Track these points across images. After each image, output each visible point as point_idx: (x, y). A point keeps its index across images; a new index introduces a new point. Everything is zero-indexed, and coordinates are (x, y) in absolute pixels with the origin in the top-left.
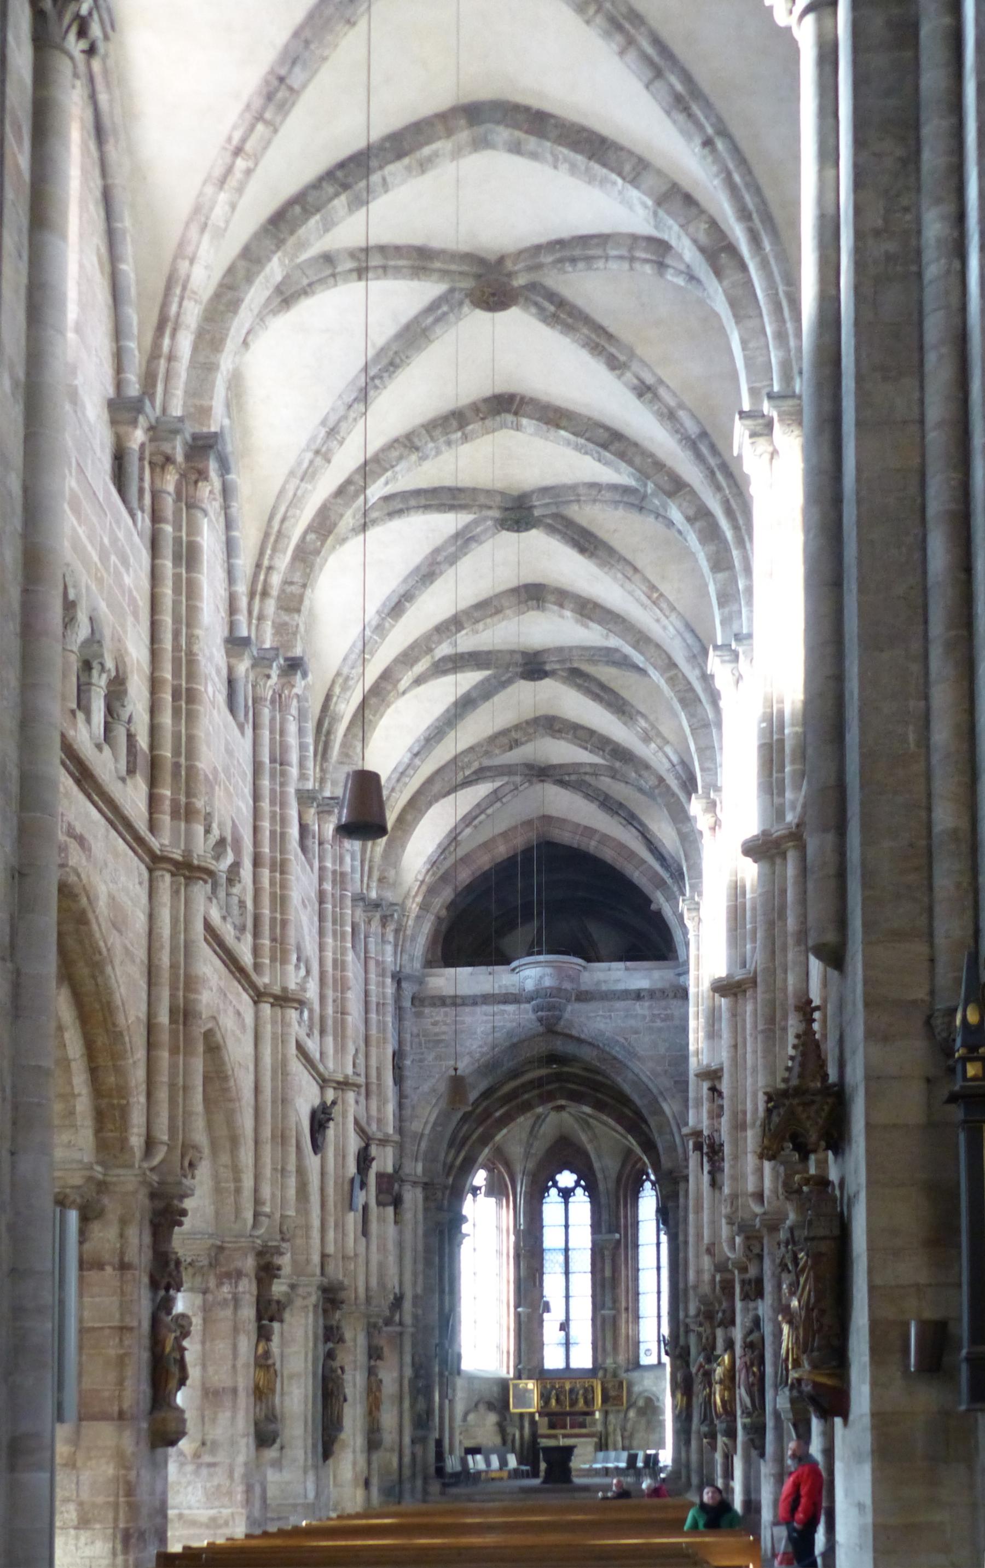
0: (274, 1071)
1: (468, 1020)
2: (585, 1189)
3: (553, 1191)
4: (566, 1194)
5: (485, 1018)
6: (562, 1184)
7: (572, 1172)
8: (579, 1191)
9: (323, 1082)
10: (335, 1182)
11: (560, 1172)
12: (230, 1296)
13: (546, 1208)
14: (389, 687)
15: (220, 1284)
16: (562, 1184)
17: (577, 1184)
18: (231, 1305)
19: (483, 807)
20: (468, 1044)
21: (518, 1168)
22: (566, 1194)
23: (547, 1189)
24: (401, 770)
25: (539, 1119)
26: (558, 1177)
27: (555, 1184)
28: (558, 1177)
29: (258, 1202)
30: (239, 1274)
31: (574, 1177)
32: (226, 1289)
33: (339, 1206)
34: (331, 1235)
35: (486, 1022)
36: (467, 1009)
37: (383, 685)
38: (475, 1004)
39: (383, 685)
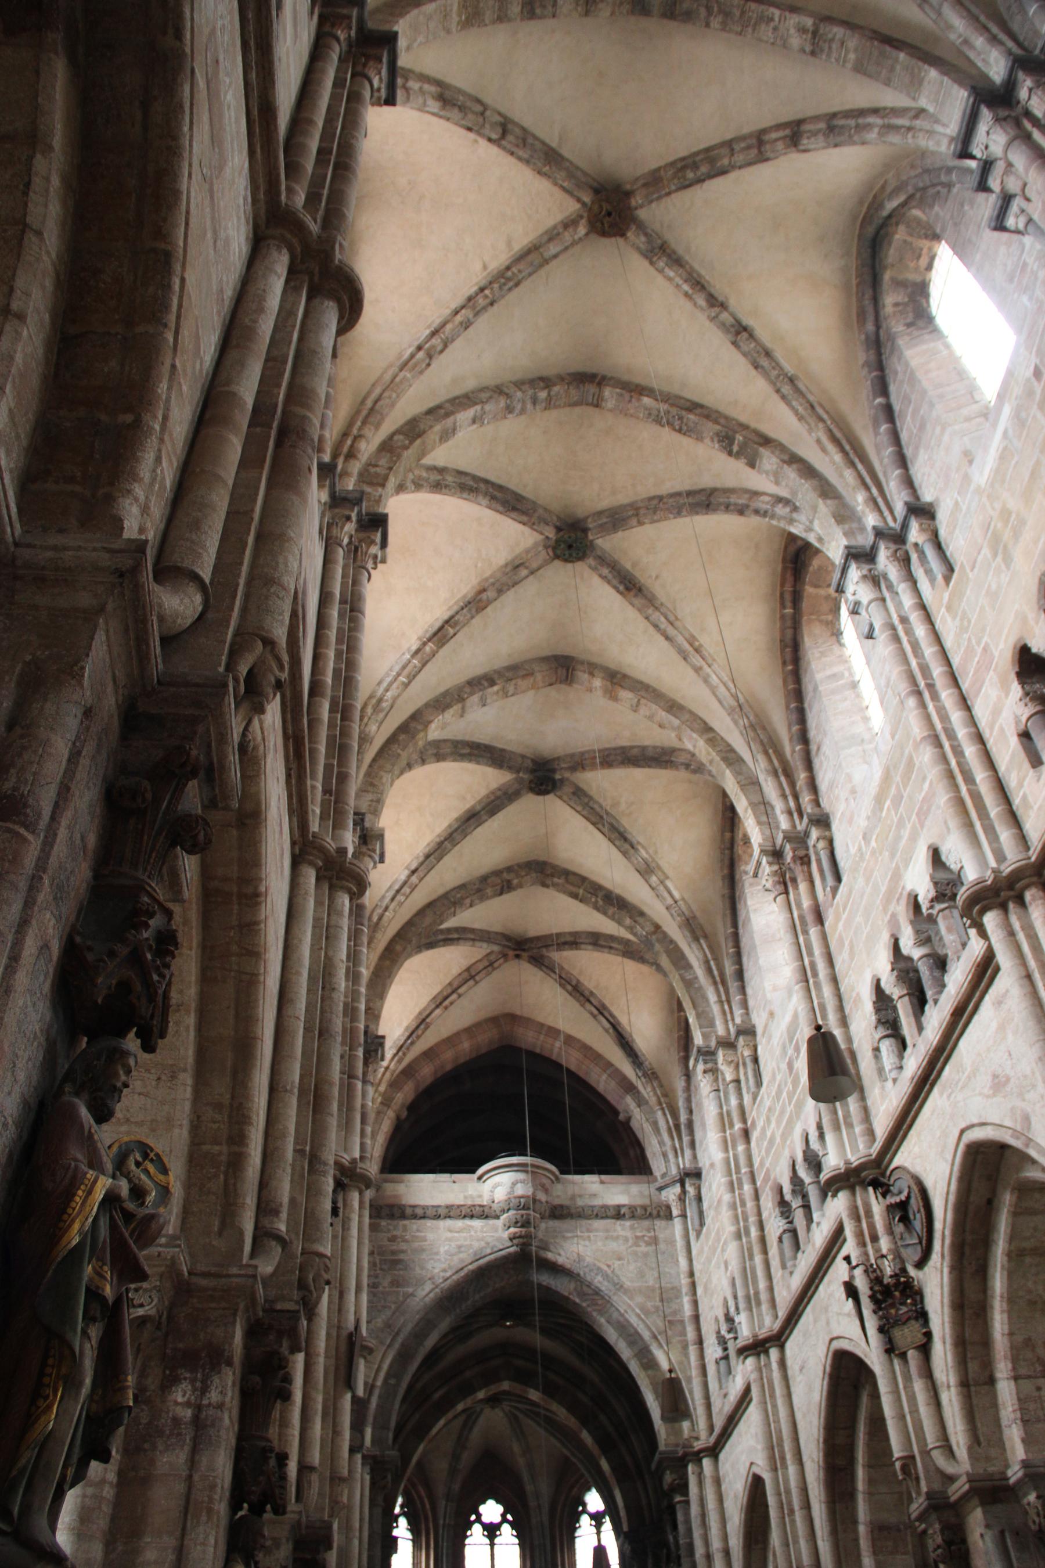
0: (312, 979)
1: (430, 1236)
2: (513, 1525)
3: (477, 1528)
4: (492, 1531)
5: (449, 1235)
6: (486, 1519)
7: (498, 1502)
8: (506, 1528)
10: (328, 1334)
11: (484, 1502)
12: (188, 1413)
13: (468, 1551)
14: (420, 727)
15: (170, 1382)
16: (486, 1519)
17: (504, 1520)
19: (455, 986)
20: (429, 1266)
21: (440, 1490)
22: (492, 1531)
23: (469, 1525)
24: (397, 887)
25: (470, 1417)
26: (482, 1509)
27: (479, 1520)
28: (482, 1509)
29: (266, 1208)
30: (217, 1358)
31: (500, 1509)
32: (181, 1394)
33: (331, 1377)
34: (317, 1428)
35: (450, 1240)
36: (429, 1223)
37: (413, 725)
38: (438, 1217)
39: (413, 725)
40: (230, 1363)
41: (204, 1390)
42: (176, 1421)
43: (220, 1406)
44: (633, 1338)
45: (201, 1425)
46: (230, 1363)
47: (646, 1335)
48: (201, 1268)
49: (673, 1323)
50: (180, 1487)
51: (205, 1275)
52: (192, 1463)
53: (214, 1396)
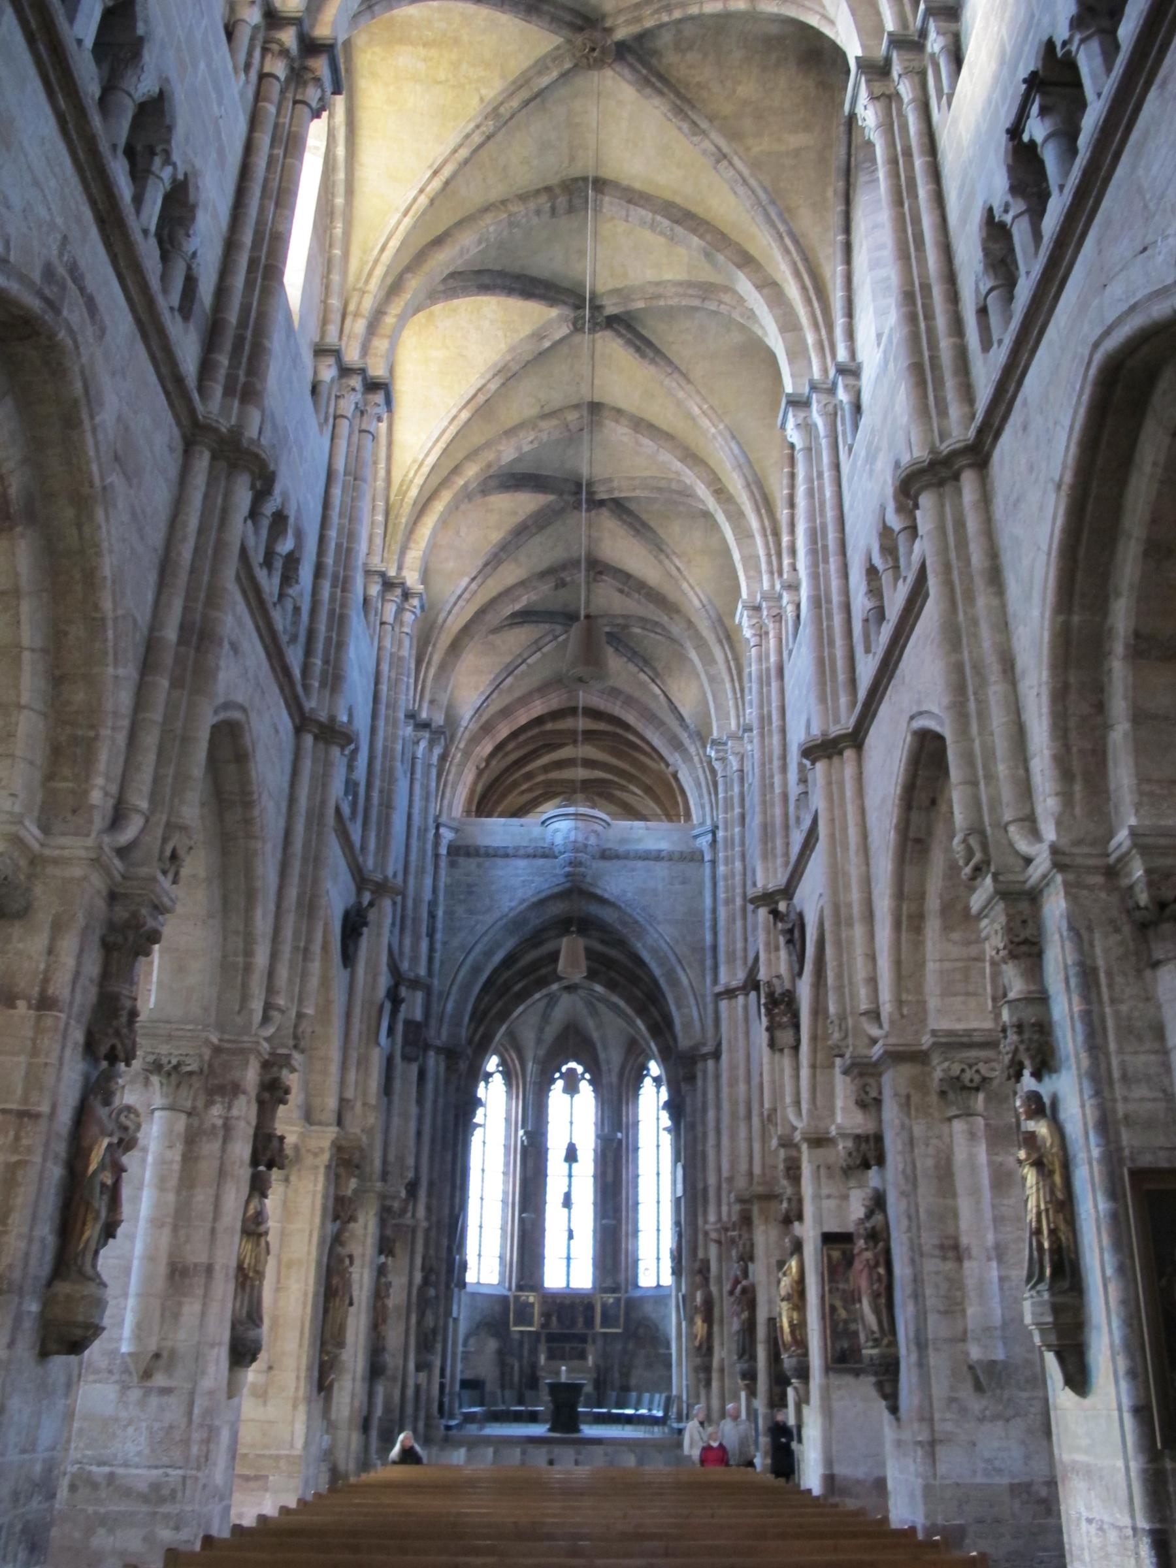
9: (360, 879)
12: (220, 1122)
15: (209, 1103)
18: (221, 1133)
30: (236, 1089)
32: (216, 1111)
40: (244, 1092)
41: (230, 1108)
42: (214, 1126)
43: (238, 1118)
44: (662, 961)
45: (227, 1127)
46: (244, 1092)
47: (673, 959)
48: (226, 1037)
49: (697, 949)
50: (217, 1163)
51: (229, 1041)
52: (223, 1150)
53: (235, 1112)
